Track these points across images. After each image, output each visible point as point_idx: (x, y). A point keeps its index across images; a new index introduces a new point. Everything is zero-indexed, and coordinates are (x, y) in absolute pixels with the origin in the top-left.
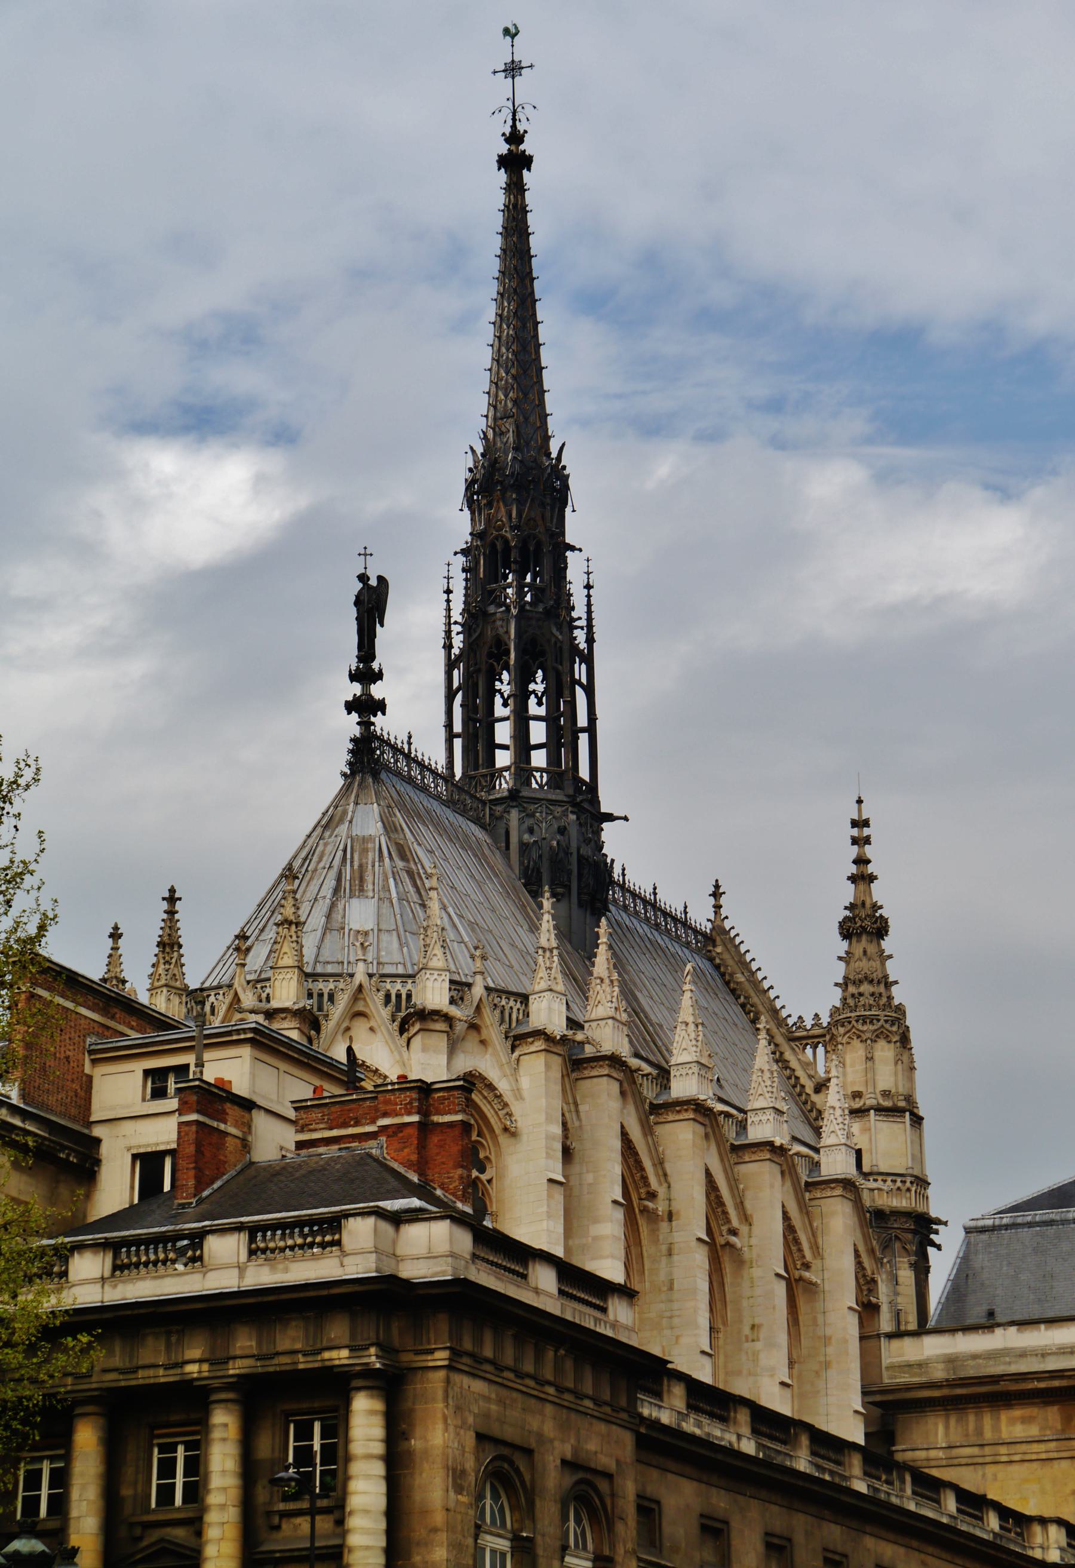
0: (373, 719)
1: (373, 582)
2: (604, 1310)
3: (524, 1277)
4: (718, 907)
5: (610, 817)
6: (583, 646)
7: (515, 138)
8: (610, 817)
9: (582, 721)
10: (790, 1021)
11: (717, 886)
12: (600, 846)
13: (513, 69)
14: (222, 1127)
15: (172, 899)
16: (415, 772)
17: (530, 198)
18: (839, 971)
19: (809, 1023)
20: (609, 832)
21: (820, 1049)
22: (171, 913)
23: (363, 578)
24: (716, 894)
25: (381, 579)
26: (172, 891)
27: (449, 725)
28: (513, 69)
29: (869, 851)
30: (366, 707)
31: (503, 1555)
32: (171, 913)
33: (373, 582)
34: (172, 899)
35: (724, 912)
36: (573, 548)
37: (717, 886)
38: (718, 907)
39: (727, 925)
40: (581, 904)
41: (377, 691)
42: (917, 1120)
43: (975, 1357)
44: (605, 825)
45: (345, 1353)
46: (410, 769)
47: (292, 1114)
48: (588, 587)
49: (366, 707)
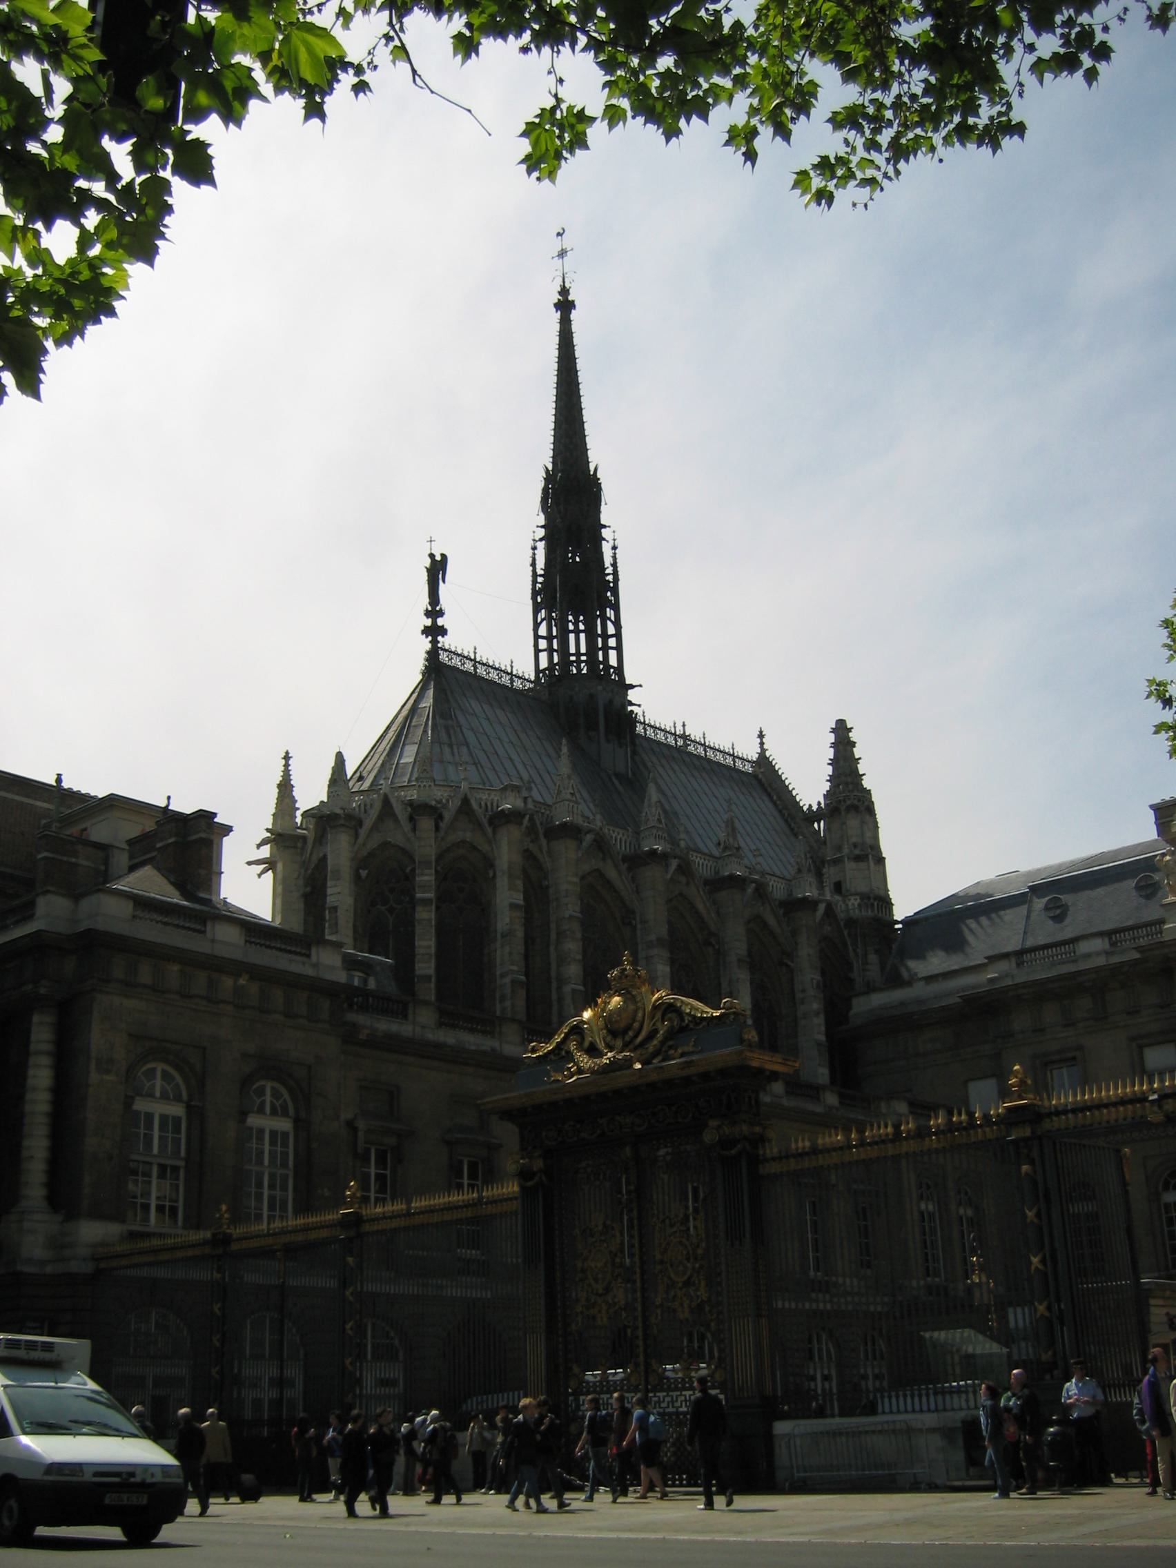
0: (440, 638)
1: (438, 558)
2: (309, 956)
3: (204, 932)
4: (762, 744)
5: (632, 687)
7: (564, 291)
8: (632, 687)
10: (805, 808)
11: (761, 732)
13: (562, 254)
14: (74, 860)
15: (287, 757)
16: (481, 671)
19: (815, 808)
20: (632, 695)
22: (287, 765)
23: (432, 556)
24: (761, 736)
26: (287, 753)
28: (562, 254)
30: (435, 632)
31: (177, 1120)
32: (287, 765)
33: (438, 558)
34: (287, 757)
36: (605, 527)
37: (761, 732)
38: (762, 744)
39: (768, 754)
40: (608, 741)
41: (440, 622)
43: (902, 1004)
44: (630, 692)
45: (30, 986)
46: (475, 668)
47: (127, 847)
48: (614, 548)
49: (435, 632)
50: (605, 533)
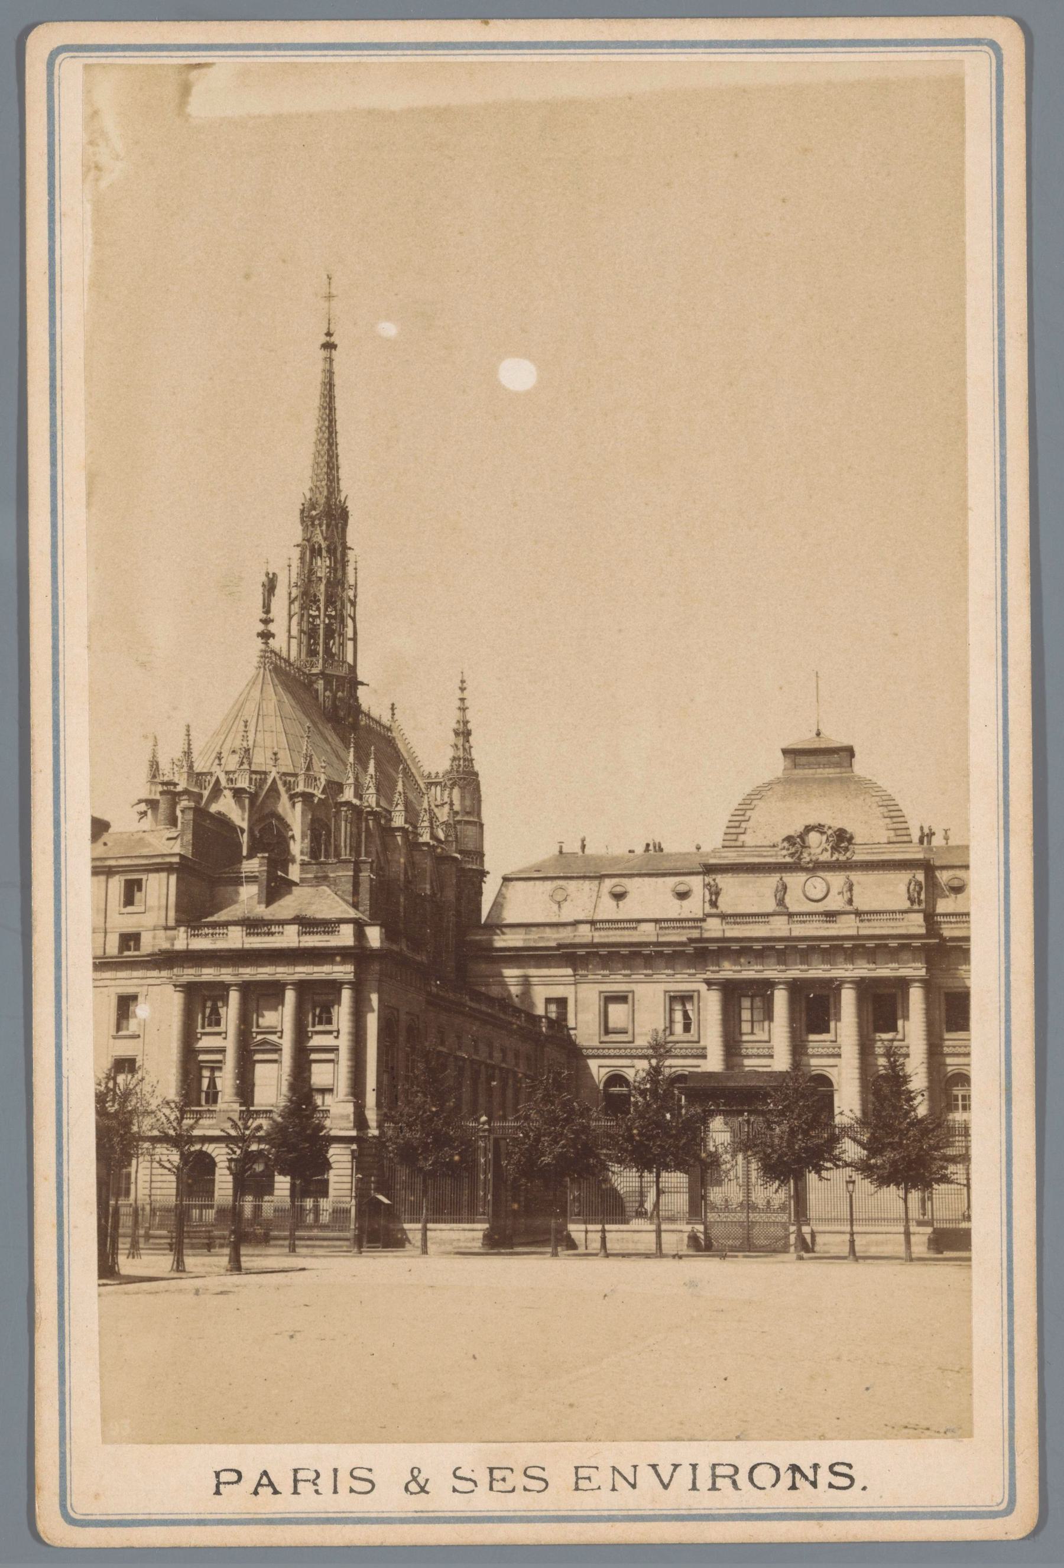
1: (271, 576)
4: (393, 714)
6: (352, 598)
8: (362, 684)
9: (350, 634)
11: (393, 705)
12: (357, 699)
17: (336, 368)
18: (451, 752)
19: (433, 776)
20: (361, 691)
21: (439, 788)
24: (393, 708)
25: (274, 574)
27: (289, 631)
28: (329, 297)
29: (466, 694)
30: (266, 636)
35: (396, 717)
37: (393, 705)
38: (393, 714)
42: (481, 826)
48: (356, 569)
50: (351, 555)
